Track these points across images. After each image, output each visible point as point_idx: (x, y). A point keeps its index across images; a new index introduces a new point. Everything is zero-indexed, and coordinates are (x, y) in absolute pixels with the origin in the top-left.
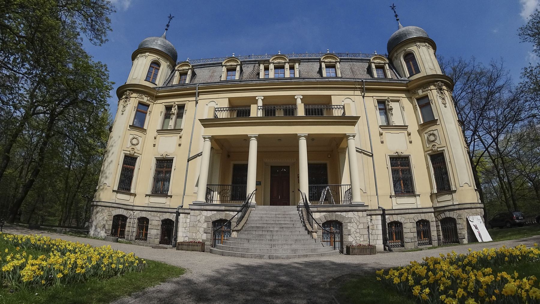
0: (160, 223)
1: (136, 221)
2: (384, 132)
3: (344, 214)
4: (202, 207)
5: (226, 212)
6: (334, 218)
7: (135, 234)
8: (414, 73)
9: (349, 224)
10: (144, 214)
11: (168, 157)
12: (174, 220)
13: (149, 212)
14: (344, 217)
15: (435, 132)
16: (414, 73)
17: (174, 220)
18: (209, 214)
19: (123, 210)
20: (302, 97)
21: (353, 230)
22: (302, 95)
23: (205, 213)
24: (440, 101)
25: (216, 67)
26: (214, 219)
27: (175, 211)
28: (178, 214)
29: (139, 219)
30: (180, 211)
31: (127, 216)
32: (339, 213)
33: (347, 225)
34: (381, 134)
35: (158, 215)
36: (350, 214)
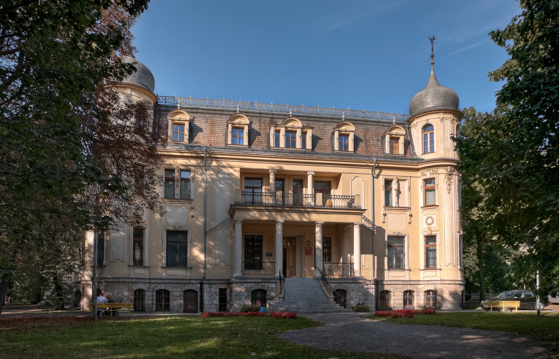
0: (182, 294)
1: (155, 294)
2: (386, 212)
3: (348, 285)
4: (244, 281)
5: (263, 284)
6: (341, 288)
7: (154, 306)
8: (429, 151)
9: (351, 292)
10: (162, 287)
11: (181, 229)
12: (198, 290)
13: (169, 284)
14: (349, 287)
15: (434, 217)
16: (429, 151)
17: (198, 290)
18: (249, 285)
19: (142, 284)
20: (314, 174)
21: (354, 296)
22: (314, 172)
23: (245, 285)
24: (445, 186)
25: (213, 116)
26: (253, 289)
27: (199, 282)
28: (202, 284)
29: (157, 292)
30: (204, 282)
31: (146, 289)
32: (345, 284)
33: (350, 293)
34: (385, 215)
35: (180, 286)
36: (353, 285)
